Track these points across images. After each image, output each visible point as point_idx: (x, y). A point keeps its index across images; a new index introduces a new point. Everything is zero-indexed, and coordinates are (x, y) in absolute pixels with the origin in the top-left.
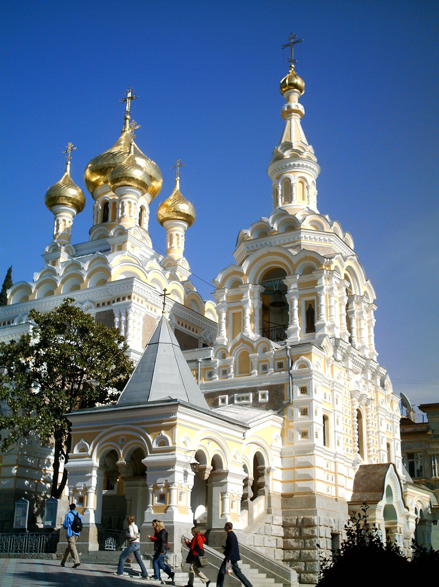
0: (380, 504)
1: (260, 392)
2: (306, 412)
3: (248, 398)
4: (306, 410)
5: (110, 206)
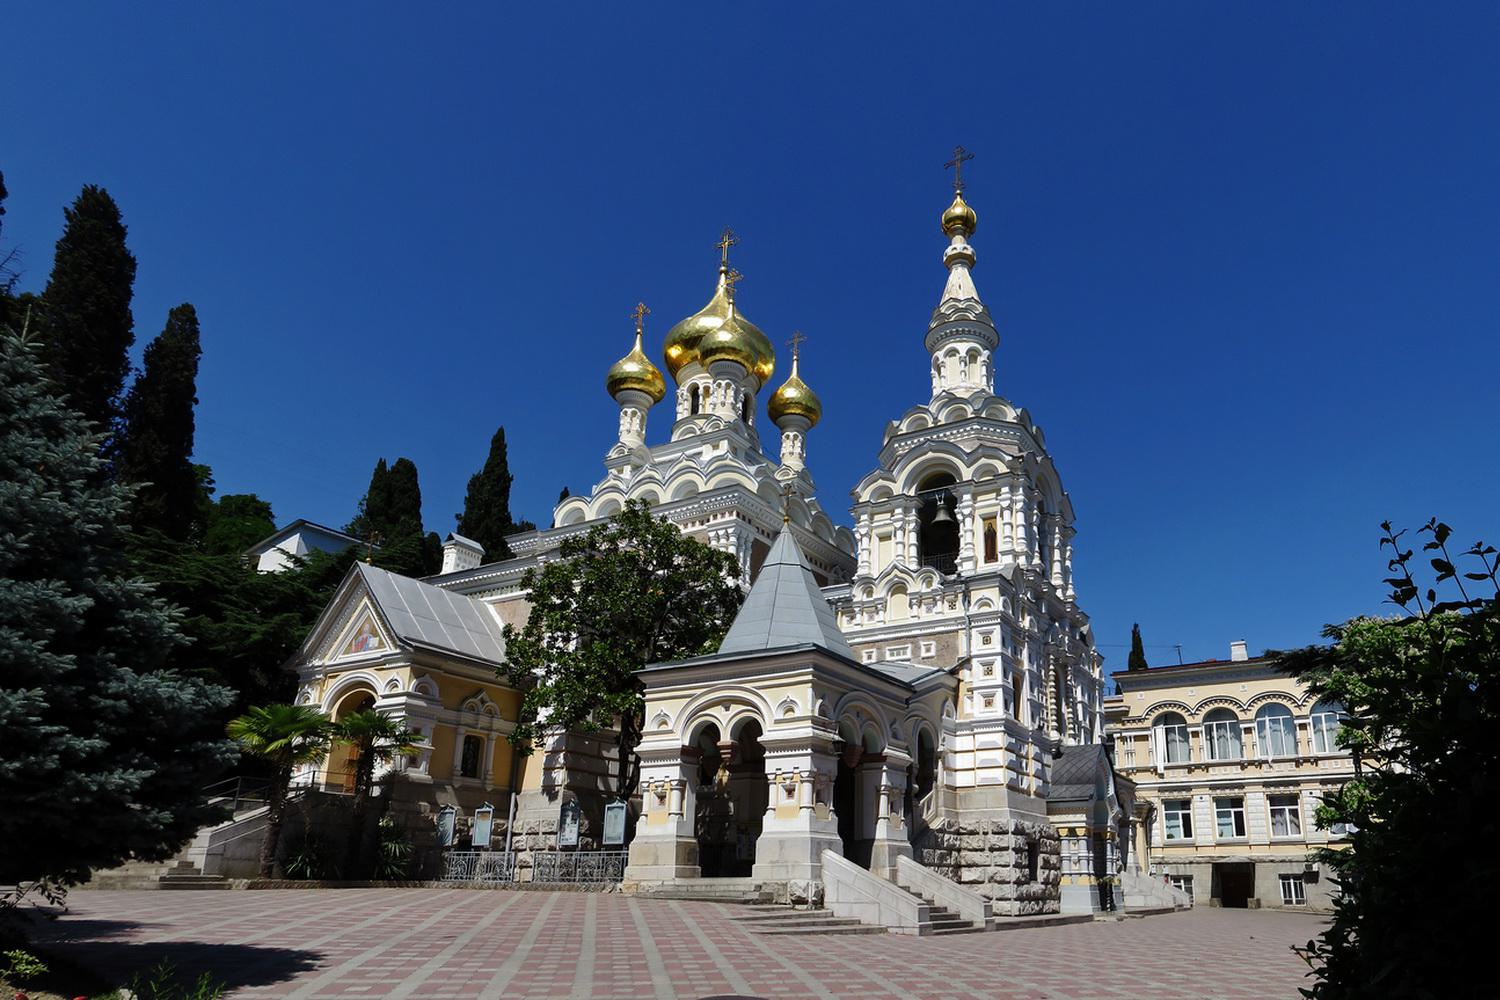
5: (701, 391)
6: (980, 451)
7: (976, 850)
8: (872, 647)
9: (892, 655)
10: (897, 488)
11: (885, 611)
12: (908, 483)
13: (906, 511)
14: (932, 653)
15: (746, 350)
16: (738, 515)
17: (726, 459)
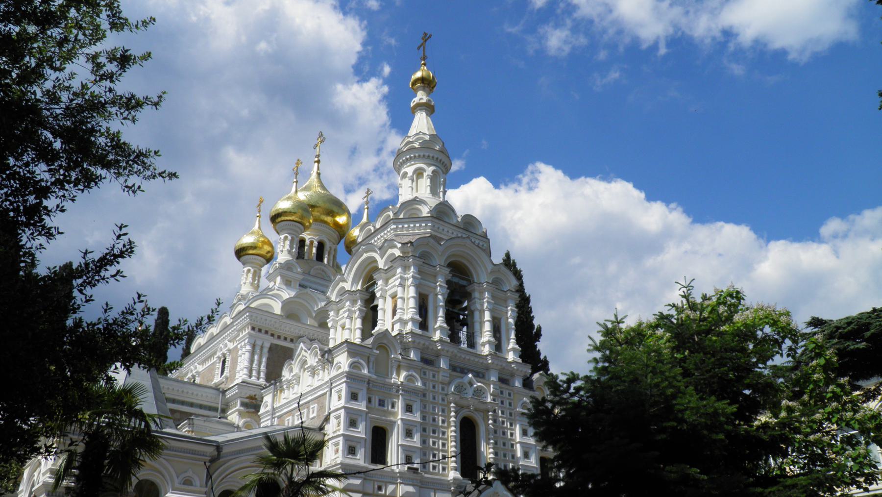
6: (386, 245)
10: (347, 286)
11: (299, 385)
12: (355, 281)
13: (354, 302)
15: (300, 212)
16: (253, 329)
17: (273, 290)
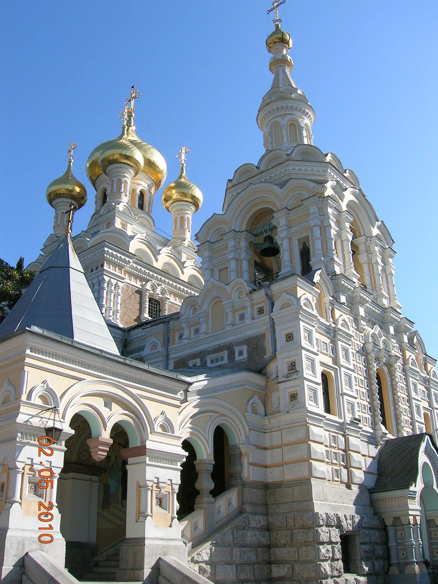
0: (412, 488)
1: (237, 349)
2: (294, 366)
3: (222, 359)
4: (293, 364)
7: (284, 546)
8: (196, 358)
9: (212, 362)
14: (245, 356)
